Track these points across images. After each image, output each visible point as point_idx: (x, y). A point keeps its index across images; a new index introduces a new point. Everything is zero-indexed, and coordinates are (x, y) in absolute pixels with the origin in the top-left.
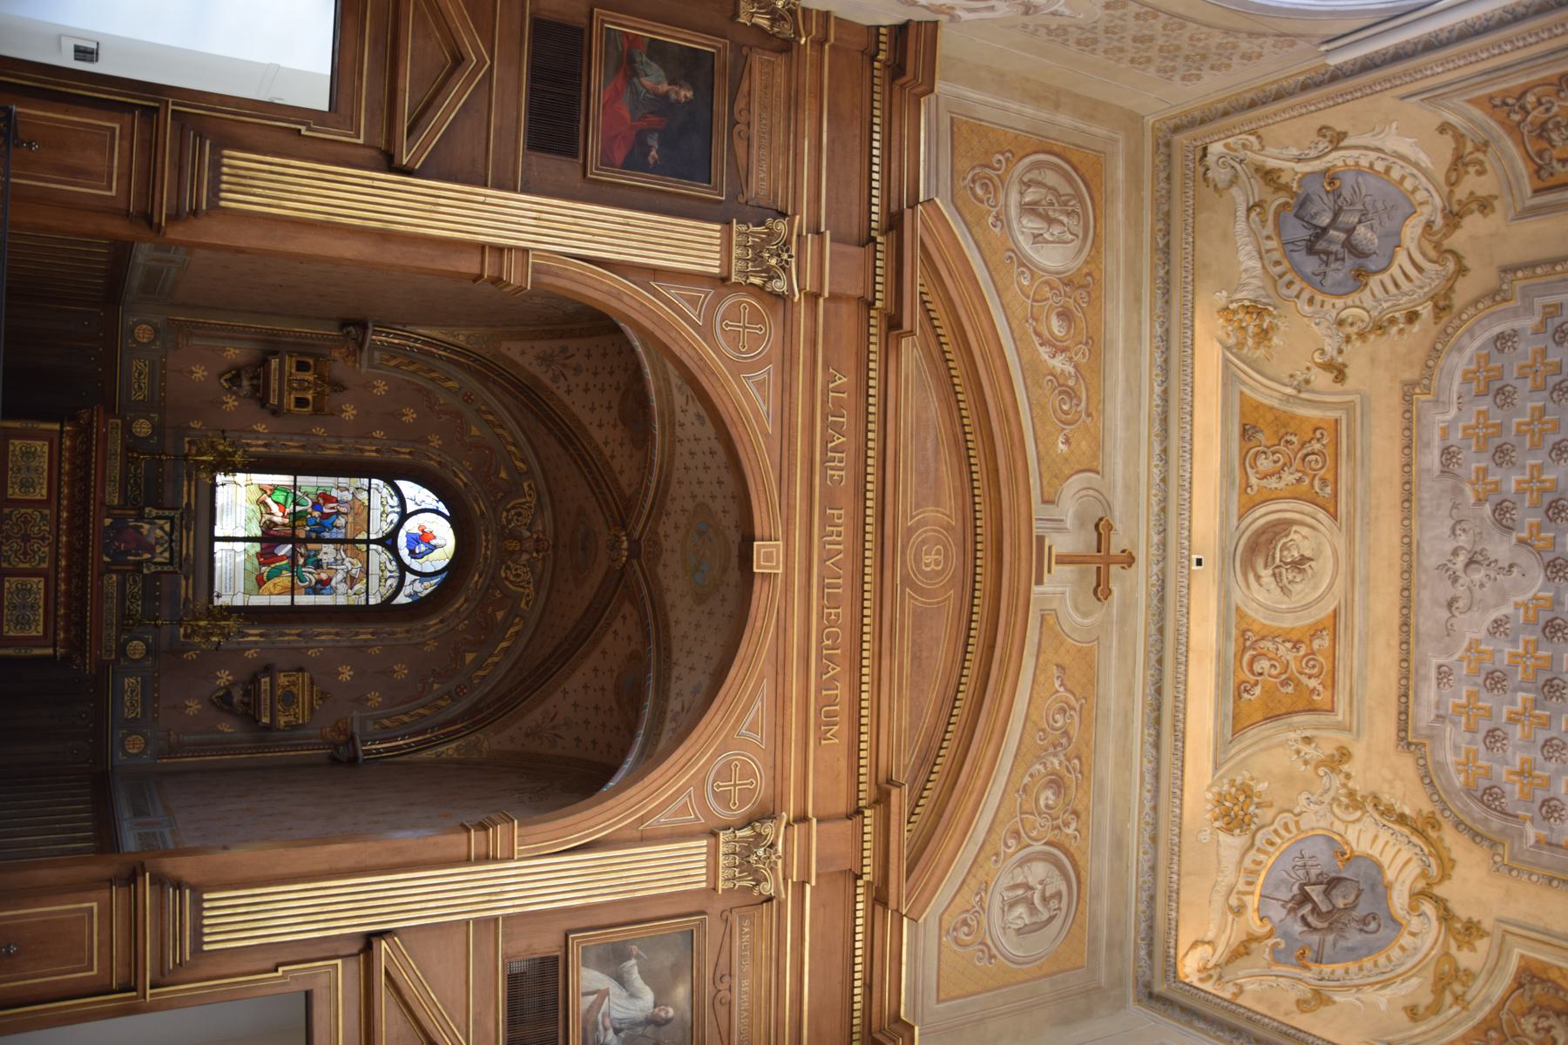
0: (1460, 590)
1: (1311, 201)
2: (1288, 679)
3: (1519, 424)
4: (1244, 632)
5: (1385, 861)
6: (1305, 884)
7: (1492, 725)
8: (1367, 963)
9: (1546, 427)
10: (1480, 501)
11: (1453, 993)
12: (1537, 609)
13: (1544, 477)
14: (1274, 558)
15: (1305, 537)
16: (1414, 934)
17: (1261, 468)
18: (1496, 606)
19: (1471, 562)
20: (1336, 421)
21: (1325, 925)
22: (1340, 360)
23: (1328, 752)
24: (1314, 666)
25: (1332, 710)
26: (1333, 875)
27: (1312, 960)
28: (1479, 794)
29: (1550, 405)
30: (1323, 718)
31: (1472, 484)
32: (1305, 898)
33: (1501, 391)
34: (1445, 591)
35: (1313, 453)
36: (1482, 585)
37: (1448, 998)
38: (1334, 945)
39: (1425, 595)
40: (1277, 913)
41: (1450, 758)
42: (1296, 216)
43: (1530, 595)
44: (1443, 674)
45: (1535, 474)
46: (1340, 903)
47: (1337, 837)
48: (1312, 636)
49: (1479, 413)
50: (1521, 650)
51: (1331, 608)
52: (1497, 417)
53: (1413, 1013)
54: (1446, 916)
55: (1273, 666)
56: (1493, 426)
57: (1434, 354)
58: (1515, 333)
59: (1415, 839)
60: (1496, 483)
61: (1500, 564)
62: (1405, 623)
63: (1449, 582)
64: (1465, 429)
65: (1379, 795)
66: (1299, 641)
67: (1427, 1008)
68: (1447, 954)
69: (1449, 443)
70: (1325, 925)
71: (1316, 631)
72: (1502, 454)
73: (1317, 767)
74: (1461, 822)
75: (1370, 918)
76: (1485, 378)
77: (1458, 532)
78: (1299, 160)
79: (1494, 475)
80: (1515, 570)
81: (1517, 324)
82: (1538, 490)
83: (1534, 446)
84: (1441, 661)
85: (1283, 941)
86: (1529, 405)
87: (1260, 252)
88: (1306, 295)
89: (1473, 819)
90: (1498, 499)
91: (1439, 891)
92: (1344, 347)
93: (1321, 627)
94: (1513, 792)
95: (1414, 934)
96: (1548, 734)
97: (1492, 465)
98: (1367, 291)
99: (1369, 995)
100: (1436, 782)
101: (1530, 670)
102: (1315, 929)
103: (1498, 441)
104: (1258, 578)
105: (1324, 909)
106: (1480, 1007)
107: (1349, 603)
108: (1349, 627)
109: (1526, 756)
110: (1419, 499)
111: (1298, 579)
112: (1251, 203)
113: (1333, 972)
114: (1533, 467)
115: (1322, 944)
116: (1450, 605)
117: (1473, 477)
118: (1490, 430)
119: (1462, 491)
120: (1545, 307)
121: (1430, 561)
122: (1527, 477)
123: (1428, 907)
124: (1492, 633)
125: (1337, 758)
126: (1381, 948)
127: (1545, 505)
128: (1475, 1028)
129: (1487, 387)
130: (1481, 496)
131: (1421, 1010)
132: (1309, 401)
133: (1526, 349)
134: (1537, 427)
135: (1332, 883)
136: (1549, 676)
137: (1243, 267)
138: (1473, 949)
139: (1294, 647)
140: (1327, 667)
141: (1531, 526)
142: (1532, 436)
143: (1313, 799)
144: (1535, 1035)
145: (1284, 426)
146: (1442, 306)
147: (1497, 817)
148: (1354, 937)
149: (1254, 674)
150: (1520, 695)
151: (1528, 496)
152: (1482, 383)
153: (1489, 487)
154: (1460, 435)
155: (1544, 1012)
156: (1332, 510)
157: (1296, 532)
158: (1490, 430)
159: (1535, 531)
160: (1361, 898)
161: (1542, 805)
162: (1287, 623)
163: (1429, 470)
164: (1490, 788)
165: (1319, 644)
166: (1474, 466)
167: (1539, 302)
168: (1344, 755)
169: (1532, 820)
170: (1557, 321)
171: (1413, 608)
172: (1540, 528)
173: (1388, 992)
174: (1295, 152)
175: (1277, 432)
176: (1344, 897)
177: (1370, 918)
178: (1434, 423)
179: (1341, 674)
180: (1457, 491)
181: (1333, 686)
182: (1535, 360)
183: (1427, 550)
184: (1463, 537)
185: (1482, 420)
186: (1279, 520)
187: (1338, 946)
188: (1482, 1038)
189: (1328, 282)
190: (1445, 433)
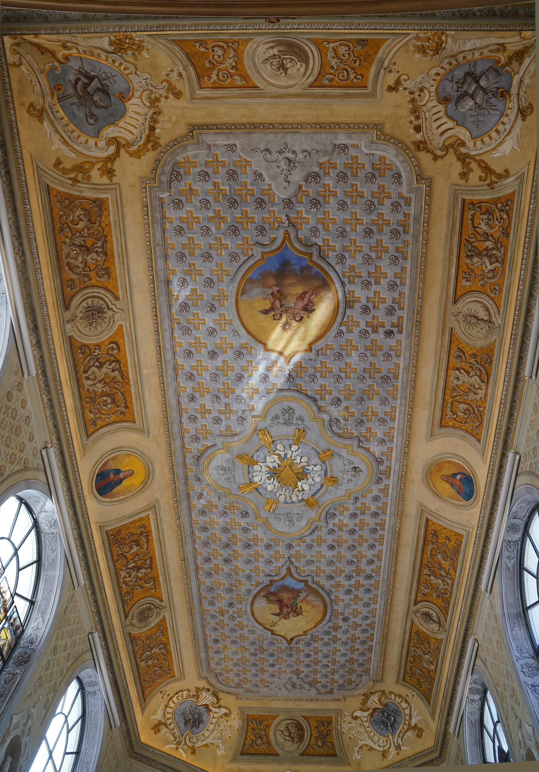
0: (275, 155)
1: (496, 76)
2: (214, 64)
3: (356, 185)
4: (237, 42)
5: (128, 120)
6: (98, 78)
7: (210, 174)
8: (72, 127)
9: (354, 198)
10: (320, 165)
11: (77, 175)
12: (269, 195)
13: (331, 197)
14: (285, 55)
15: (299, 70)
16: (96, 144)
17: (340, 48)
18: (269, 175)
19: (290, 161)
20: (366, 87)
21: (81, 94)
22: (401, 88)
23: (177, 86)
24: (224, 77)
25: (201, 88)
26: (110, 92)
27: (58, 95)
28: (176, 169)
29: (364, 200)
30: (195, 83)
31: (329, 160)
32: (91, 79)
33: (374, 176)
34: (274, 148)
35: (348, 74)
36: (278, 167)
37: (72, 175)
38: (72, 104)
39: (271, 137)
40: (75, 64)
41: (190, 153)
42: (491, 67)
43: (275, 192)
44: (232, 148)
45: (332, 193)
46: (96, 98)
47: (131, 94)
48: (241, 75)
49: (364, 165)
50: (249, 187)
51: (259, 85)
52: (361, 174)
53: (58, 163)
54: (111, 159)
55: (220, 57)
56: (357, 172)
57: (397, 142)
58: (401, 184)
59: (144, 137)
60: (329, 174)
61: (289, 176)
62: (254, 126)
63: (279, 150)
64: (357, 157)
65: (161, 115)
66: (237, 69)
67: (64, 169)
68: (93, 164)
69: (350, 148)
70: (81, 94)
71: (245, 77)
72: (342, 177)
73: (166, 81)
74: (159, 162)
75: (95, 118)
76: (381, 168)
77: (304, 153)
78: (521, 81)
79: (333, 172)
80: (287, 184)
81: (404, 185)
82: (325, 195)
83: (346, 192)
84: (238, 146)
85: (60, 72)
86: (365, 190)
87: (474, 49)
88: (442, 71)
89: (163, 167)
90: (321, 174)
91: (122, 151)
92: (408, 90)
93: (247, 79)
94: (181, 186)
95: (96, 144)
96: (212, 201)
97: (337, 171)
98: (437, 104)
99: (56, 138)
100: (175, 147)
101: (240, 192)
102: (75, 88)
103: (349, 175)
104: (272, 48)
105: (89, 89)
106: (76, 191)
107: (264, 96)
108: (249, 96)
109: (200, 191)
110: (321, 133)
111: (273, 67)
112: (506, 45)
113: (58, 111)
114: (336, 192)
115: (69, 96)
116: (267, 150)
117: (332, 161)
118: (355, 170)
119: (325, 155)
120: (410, 198)
121: (289, 139)
122: (331, 189)
123: (112, 149)
124: (255, 173)
125: (175, 91)
126: (82, 131)
127: (317, 198)
128: (66, 193)
129: (377, 169)
130: (322, 166)
131: (61, 167)
132: (379, 73)
133: (392, 189)
134: (355, 194)
135: (104, 91)
136: (238, 201)
137: (467, 41)
138: (101, 176)
139: (233, 67)
140: (225, 84)
141: (308, 192)
142: (350, 192)
143: (148, 81)
144: (76, 217)
145: (365, 59)
146: (421, 146)
147: (167, 179)
148: (81, 114)
149: (212, 48)
150: (227, 188)
151: (323, 190)
152: (378, 166)
153: (327, 170)
154: (353, 154)
155: (87, 215)
156: (315, 84)
157: (302, 65)
158: (355, 170)
159: (305, 193)
160: (103, 109)
161: (179, 200)
162: (247, 62)
163: (336, 138)
164: (180, 175)
165: (237, 79)
166: (338, 161)
167: (413, 196)
168: (178, 95)
169: (170, 195)
170: (403, 204)
171: (264, 131)
172: (307, 196)
173: (62, 146)
174: (527, 81)
175: (362, 55)
176: (100, 100)
177: (95, 118)
178: (361, 140)
179: (222, 92)
180: (325, 153)
181: (214, 88)
182: (386, 193)
183: (294, 137)
184: (302, 156)
185: (360, 166)
186: (309, 57)
187: (72, 106)
188: (63, 199)
189: (447, 83)
190: (355, 146)
